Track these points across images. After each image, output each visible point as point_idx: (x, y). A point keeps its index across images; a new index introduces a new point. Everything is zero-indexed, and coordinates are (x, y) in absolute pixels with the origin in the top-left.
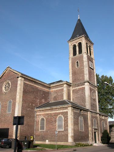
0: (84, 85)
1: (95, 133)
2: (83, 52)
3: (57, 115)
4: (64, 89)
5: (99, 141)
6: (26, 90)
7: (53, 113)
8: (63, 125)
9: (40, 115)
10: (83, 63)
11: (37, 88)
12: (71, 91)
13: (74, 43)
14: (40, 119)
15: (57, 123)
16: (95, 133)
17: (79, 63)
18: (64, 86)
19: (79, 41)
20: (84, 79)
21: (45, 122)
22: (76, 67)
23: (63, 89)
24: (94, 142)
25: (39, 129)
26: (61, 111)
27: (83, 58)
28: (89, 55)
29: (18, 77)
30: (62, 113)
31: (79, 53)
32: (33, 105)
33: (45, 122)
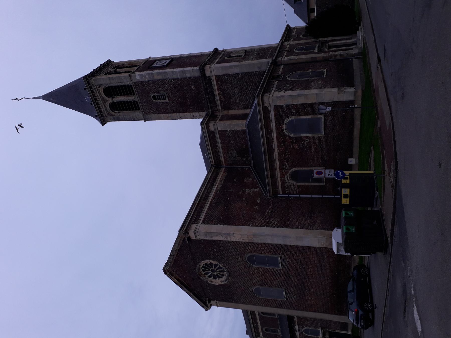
0: (209, 78)
1: (330, 47)
2: (128, 83)
3: (285, 136)
4: (220, 129)
5: (352, 49)
6: (221, 218)
7: (279, 147)
8: (309, 117)
9: (283, 182)
10: (155, 81)
11: (216, 193)
12: (225, 112)
13: (106, 109)
14: (293, 182)
15: (303, 135)
16: (330, 47)
17: (156, 94)
18: (213, 129)
19: (100, 94)
20: (196, 78)
21: (301, 169)
22: (167, 100)
23: (221, 133)
24: (354, 46)
25: (322, 184)
26: (274, 124)
27: (144, 82)
28: (136, 68)
29: (189, 238)
30: (279, 121)
31: (136, 110)
32: (258, 201)
33: (301, 169)
